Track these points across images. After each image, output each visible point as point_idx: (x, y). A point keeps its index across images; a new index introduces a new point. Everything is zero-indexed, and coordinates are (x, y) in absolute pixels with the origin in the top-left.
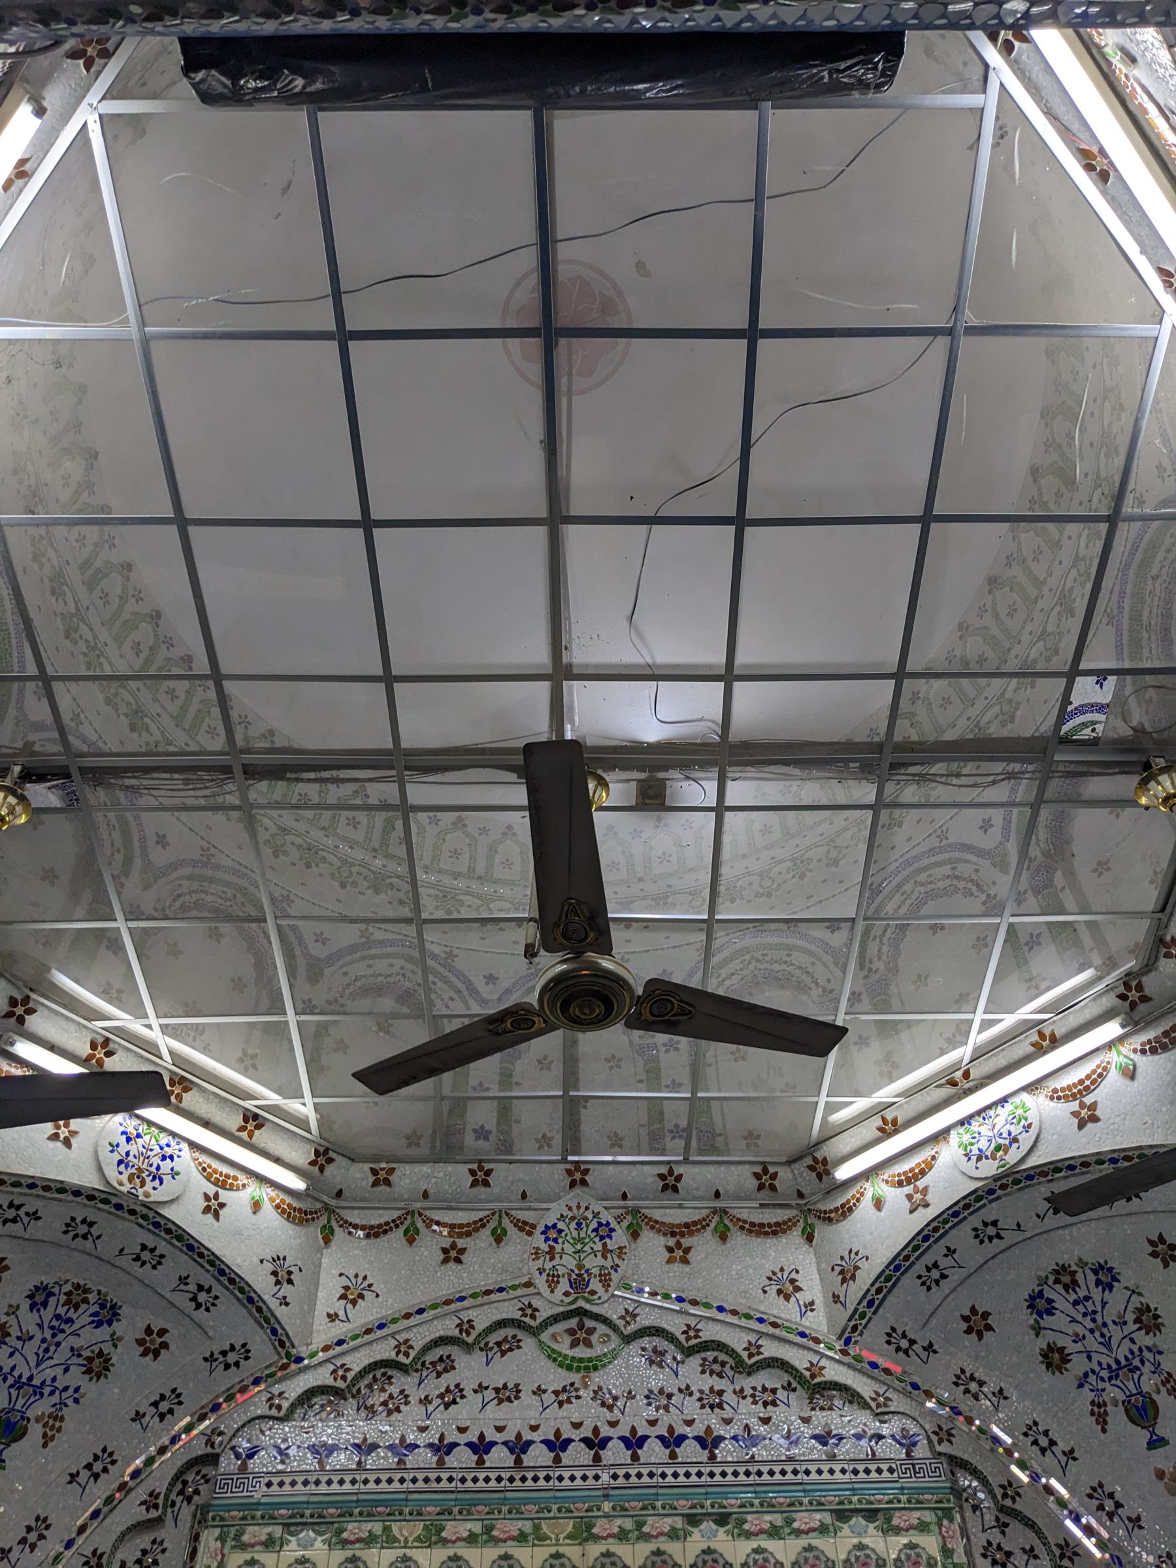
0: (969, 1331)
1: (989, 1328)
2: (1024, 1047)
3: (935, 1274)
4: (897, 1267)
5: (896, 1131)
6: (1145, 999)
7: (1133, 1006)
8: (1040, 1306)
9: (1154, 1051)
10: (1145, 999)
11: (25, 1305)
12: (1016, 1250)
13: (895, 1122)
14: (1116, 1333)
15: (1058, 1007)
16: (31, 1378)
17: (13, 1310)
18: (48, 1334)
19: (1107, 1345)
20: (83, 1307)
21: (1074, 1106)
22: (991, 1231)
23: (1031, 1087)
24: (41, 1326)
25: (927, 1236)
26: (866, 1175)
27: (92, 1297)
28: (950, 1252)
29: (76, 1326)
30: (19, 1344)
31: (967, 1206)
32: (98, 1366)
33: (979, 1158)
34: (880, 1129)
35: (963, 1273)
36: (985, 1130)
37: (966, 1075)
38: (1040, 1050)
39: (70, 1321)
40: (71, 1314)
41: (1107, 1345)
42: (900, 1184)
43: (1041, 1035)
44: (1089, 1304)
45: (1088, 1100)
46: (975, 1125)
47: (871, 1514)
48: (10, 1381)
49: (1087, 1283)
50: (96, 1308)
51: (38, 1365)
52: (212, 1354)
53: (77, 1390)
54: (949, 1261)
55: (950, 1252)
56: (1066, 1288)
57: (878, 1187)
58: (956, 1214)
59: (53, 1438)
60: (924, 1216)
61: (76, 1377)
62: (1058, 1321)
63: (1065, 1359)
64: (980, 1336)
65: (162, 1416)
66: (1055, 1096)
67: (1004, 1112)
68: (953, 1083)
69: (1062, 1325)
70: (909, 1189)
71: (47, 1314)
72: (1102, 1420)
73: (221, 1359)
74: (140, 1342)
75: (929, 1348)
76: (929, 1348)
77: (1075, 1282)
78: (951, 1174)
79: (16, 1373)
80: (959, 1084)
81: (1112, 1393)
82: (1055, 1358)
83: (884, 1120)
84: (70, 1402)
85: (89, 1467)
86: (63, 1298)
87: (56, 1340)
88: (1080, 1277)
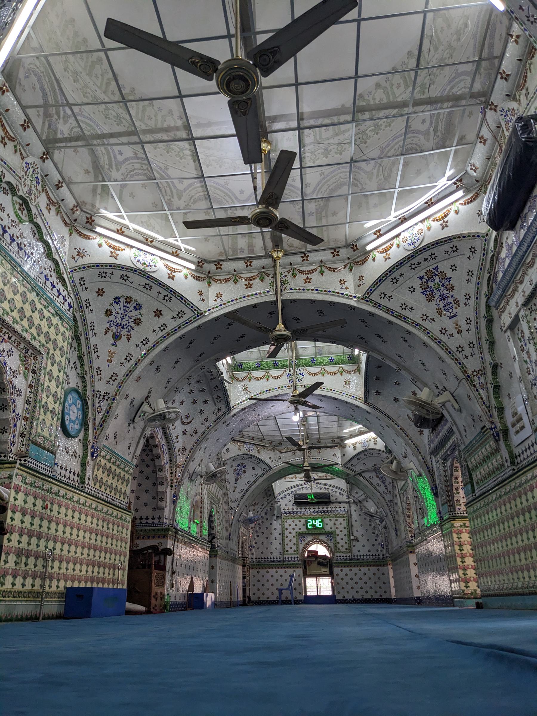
0: (97, 292)
1: (102, 295)
2: (170, 250)
3: (104, 275)
4: (97, 266)
5: (121, 234)
6: (201, 267)
7: (198, 266)
8: (117, 300)
9: (194, 278)
10: (201, 267)
12: (125, 286)
13: (123, 232)
14: (127, 318)
15: (187, 251)
19: (122, 319)
21: (170, 272)
22: (125, 278)
23: (162, 258)
25: (111, 265)
26: (100, 235)
28: (112, 273)
31: (127, 269)
33: (138, 261)
34: (118, 230)
35: (110, 280)
36: (143, 256)
37: (152, 242)
38: (173, 254)
41: (122, 319)
42: (110, 247)
43: (176, 252)
44: (127, 309)
45: (173, 274)
46: (141, 252)
47: (61, 318)
49: (132, 306)
54: (110, 275)
55: (112, 273)
56: (126, 302)
57: (102, 241)
58: (123, 268)
60: (112, 261)
62: (117, 306)
63: (110, 315)
64: (99, 295)
66: (166, 265)
67: (151, 257)
68: (147, 240)
69: (117, 308)
70: (113, 250)
72: (106, 332)
75: (86, 289)
76: (86, 289)
77: (129, 303)
78: (128, 256)
80: (148, 241)
81: (113, 329)
82: (108, 313)
83: (121, 229)
88: (132, 303)
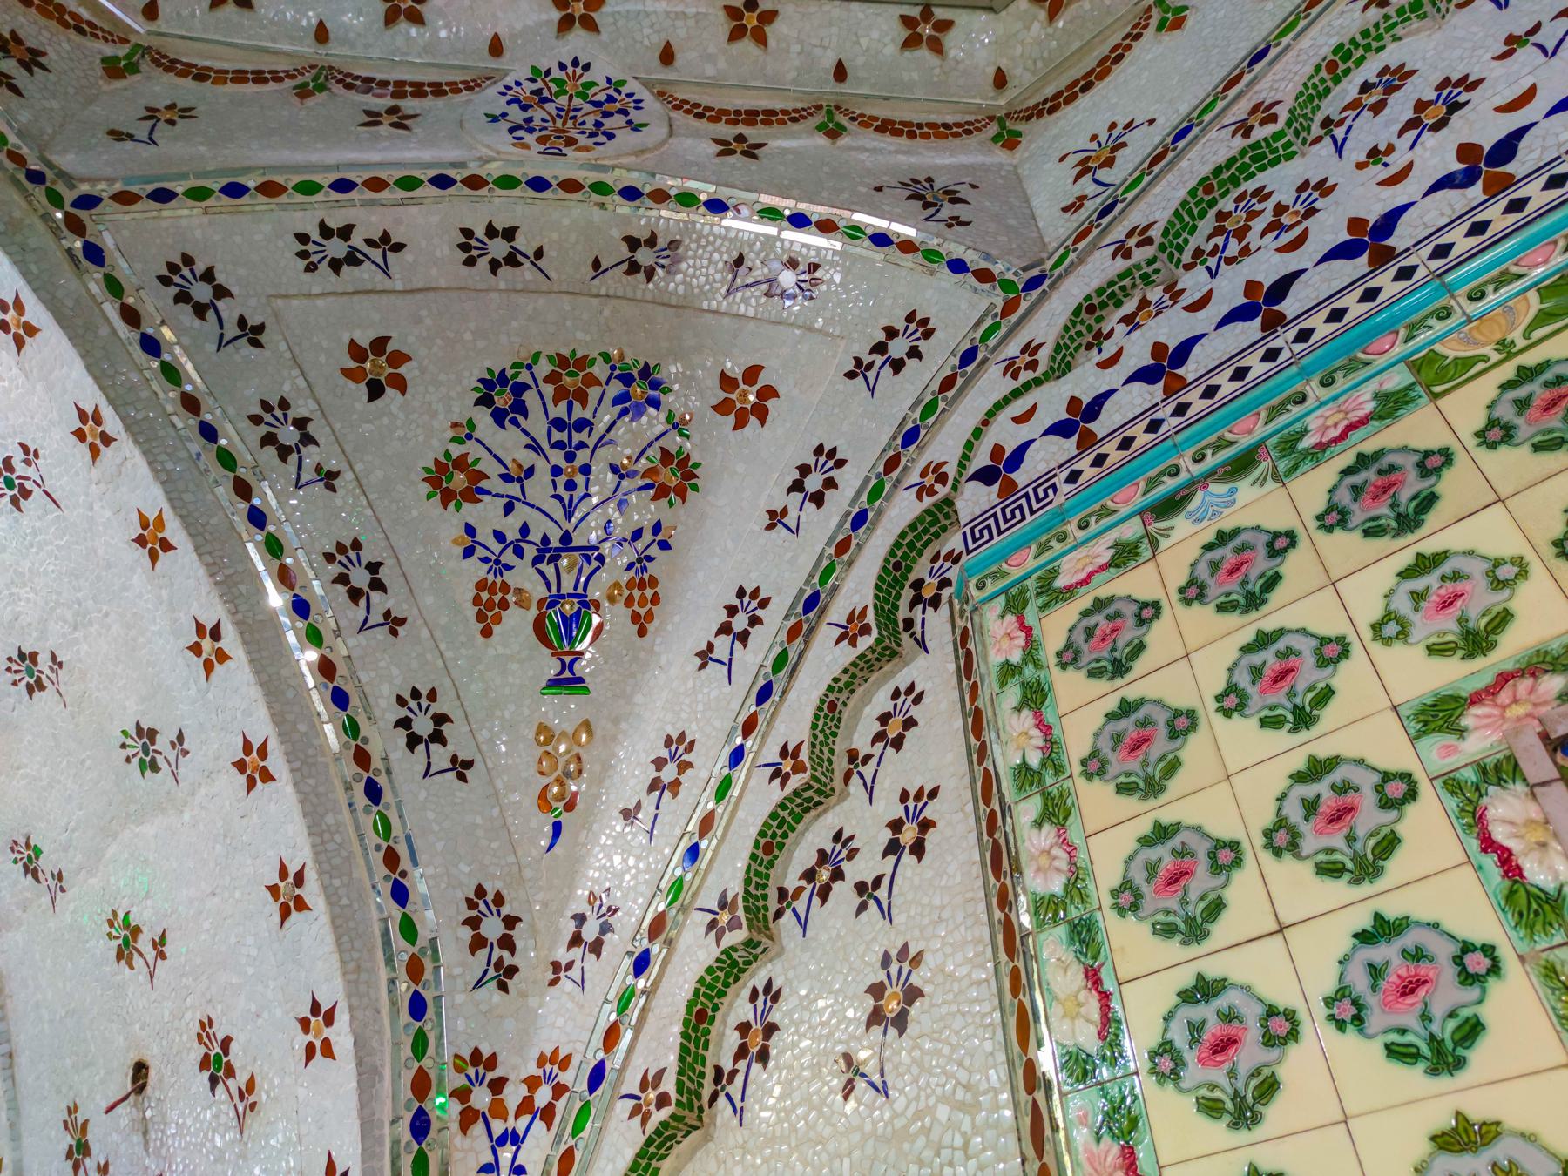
11: (483, 418)
16: (566, 538)
17: (465, 431)
18: (557, 458)
20: (594, 393)
24: (535, 447)
27: (600, 370)
29: (600, 428)
30: (513, 490)
32: (675, 476)
39: (583, 424)
40: (578, 412)
48: (530, 552)
50: (616, 388)
51: (569, 515)
52: (858, 361)
53: (657, 528)
59: (650, 616)
61: (644, 510)
65: (818, 499)
71: (537, 424)
73: (879, 359)
74: (722, 408)
79: (535, 536)
84: (654, 551)
85: (725, 629)
86: (548, 390)
87: (578, 463)
